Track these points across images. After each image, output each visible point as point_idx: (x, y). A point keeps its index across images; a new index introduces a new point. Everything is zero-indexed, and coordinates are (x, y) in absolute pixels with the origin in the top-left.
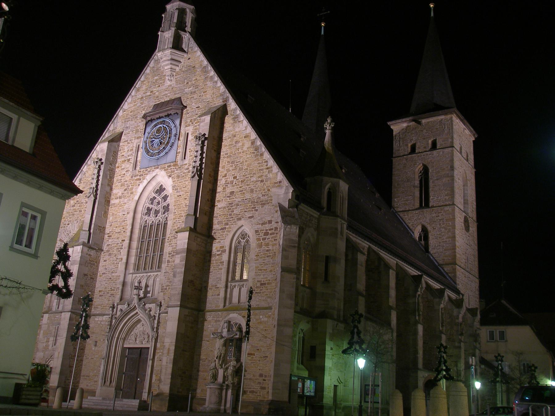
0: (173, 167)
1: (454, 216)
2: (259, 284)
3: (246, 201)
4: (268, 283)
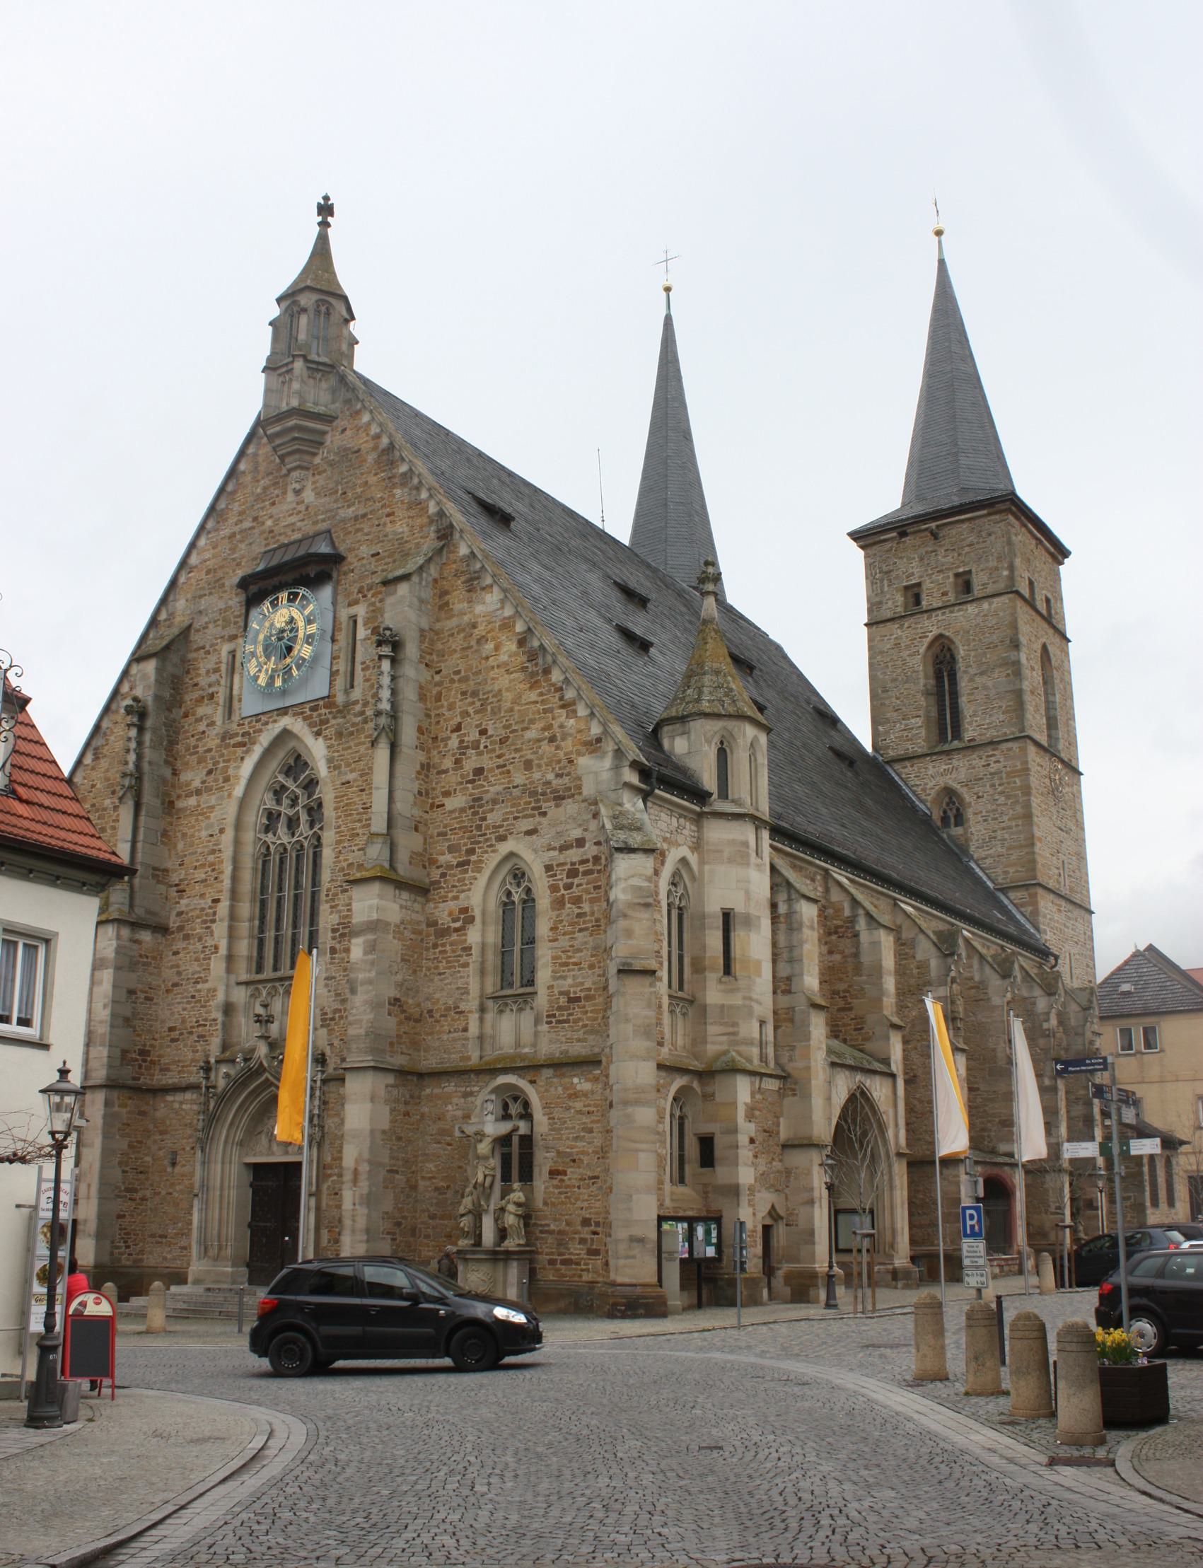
0: (323, 711)
1: (1027, 762)
2: (563, 1000)
3: (516, 792)
4: (588, 998)
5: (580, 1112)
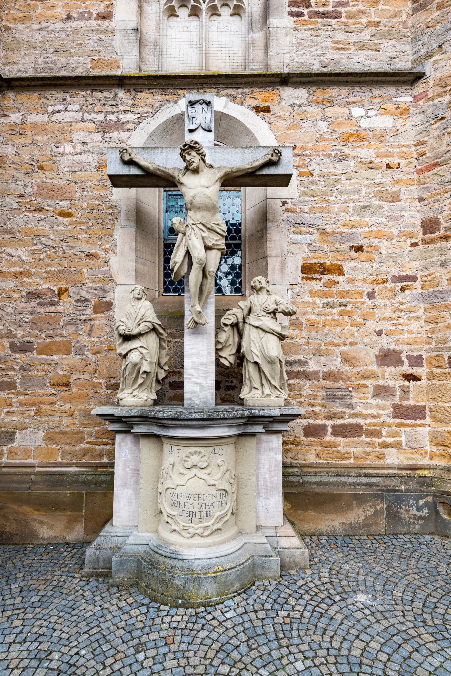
5: (370, 166)
